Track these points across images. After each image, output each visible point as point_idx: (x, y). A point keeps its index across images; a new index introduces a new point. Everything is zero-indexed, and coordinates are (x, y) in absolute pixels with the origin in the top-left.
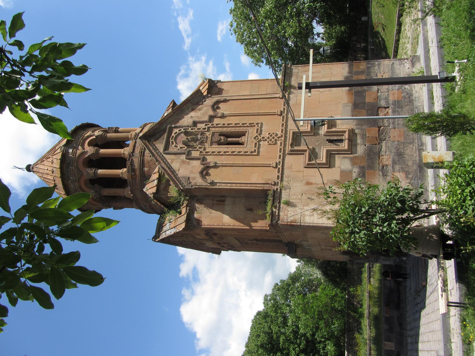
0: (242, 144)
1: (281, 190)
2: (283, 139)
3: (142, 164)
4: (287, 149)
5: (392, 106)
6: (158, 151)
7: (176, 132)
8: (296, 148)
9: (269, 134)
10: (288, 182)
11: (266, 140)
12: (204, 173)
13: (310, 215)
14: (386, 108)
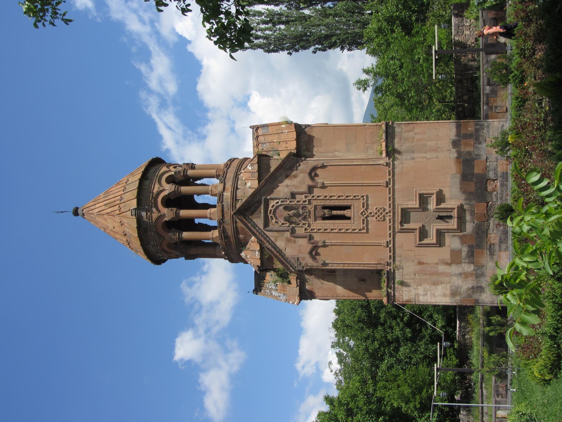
0: (349, 218)
1: (394, 270)
2: (391, 214)
3: (236, 231)
4: (396, 225)
5: (501, 179)
6: (257, 228)
7: (273, 206)
8: (406, 226)
9: (376, 209)
10: (400, 261)
11: (374, 216)
12: (314, 252)
13: (423, 295)
14: (494, 180)
